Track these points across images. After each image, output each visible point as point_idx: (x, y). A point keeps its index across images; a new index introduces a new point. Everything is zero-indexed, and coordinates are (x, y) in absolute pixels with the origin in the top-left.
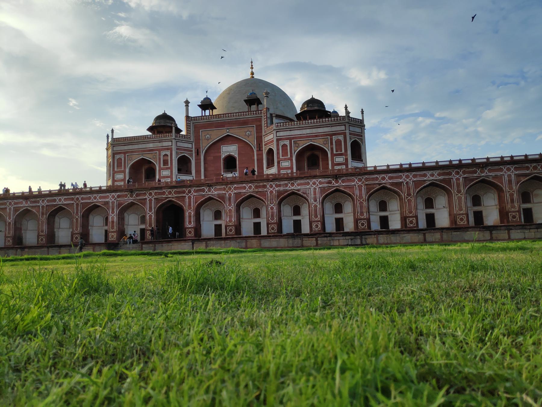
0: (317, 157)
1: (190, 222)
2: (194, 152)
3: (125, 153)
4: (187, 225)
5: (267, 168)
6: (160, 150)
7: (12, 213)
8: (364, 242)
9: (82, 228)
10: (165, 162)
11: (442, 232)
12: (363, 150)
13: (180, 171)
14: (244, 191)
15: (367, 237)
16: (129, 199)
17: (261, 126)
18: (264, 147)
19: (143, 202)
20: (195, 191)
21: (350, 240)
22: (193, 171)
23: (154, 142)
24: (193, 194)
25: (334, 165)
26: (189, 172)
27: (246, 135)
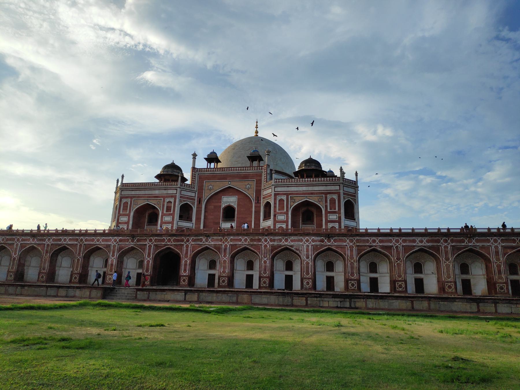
0: (313, 213)
1: (185, 270)
2: (196, 200)
3: (131, 198)
4: (182, 273)
5: (264, 220)
6: (164, 197)
8: (353, 306)
9: (82, 269)
11: (430, 301)
12: (355, 210)
13: (181, 217)
15: (356, 300)
16: (130, 244)
17: (261, 180)
18: (262, 200)
20: (193, 240)
21: (339, 302)
22: (194, 219)
23: (159, 189)
25: (327, 222)
26: (189, 219)
27: (246, 188)
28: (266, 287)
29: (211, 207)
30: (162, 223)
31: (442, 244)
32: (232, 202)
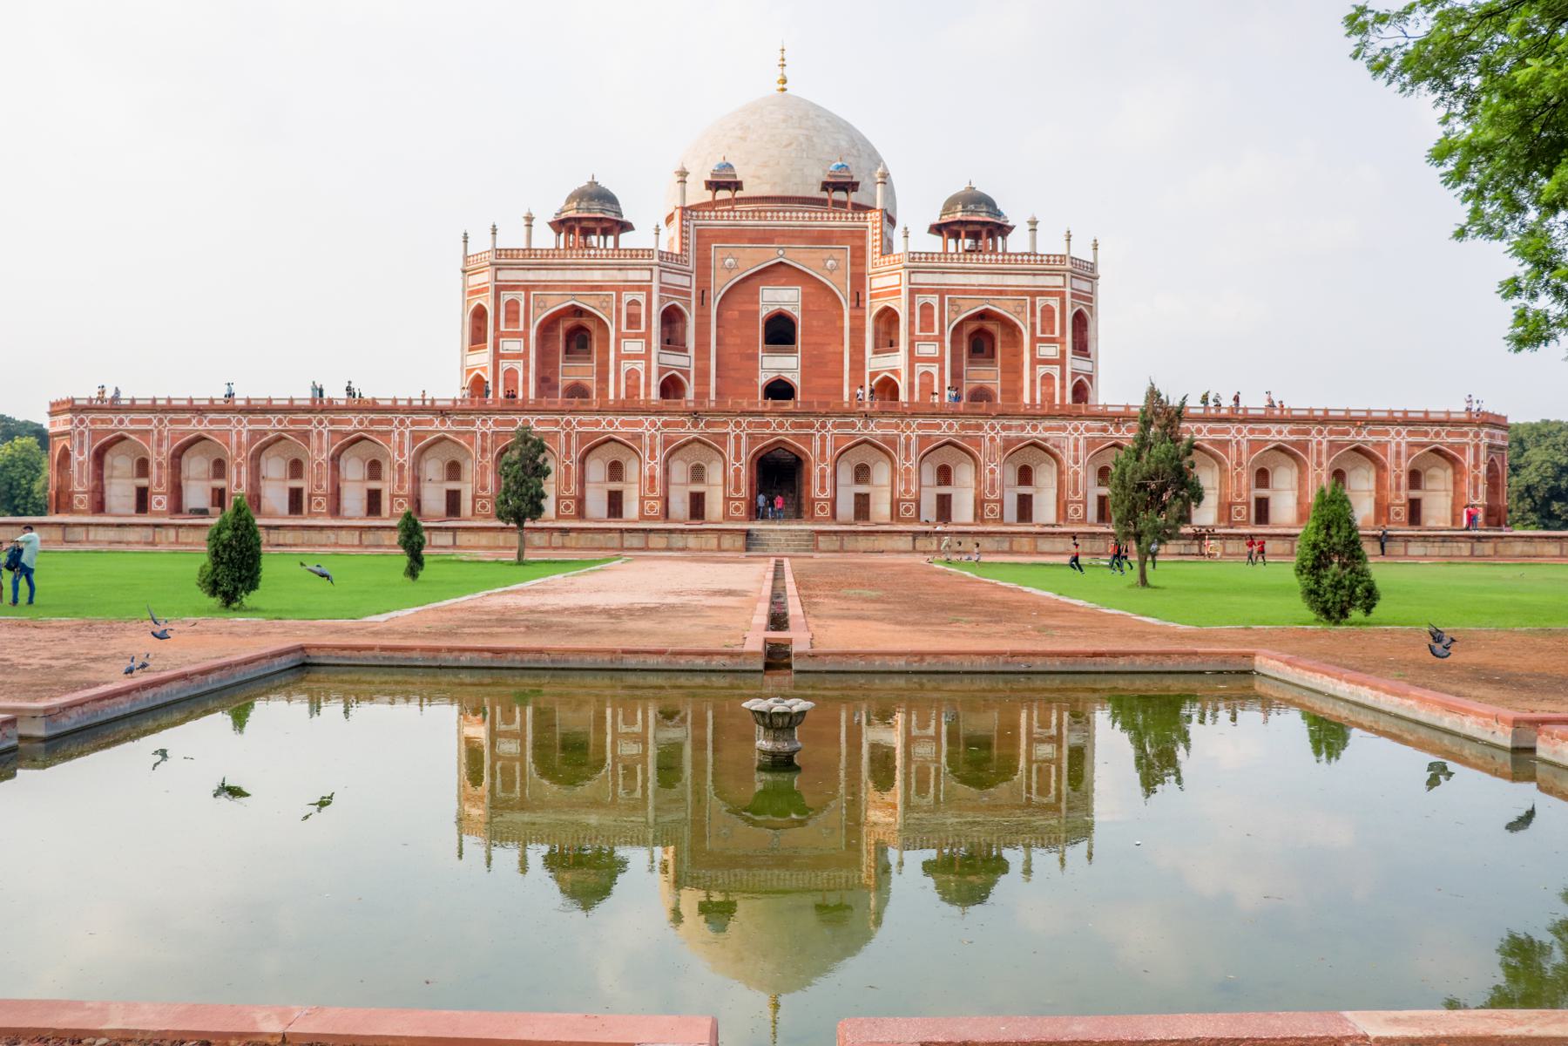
0: (991, 337)
1: (823, 489)
3: (527, 289)
4: (815, 492)
5: (875, 353)
6: (619, 290)
7: (407, 442)
10: (633, 321)
12: (1091, 333)
17: (863, 249)
18: (868, 301)
20: (835, 426)
23: (603, 267)
24: (831, 432)
25: (1035, 362)
26: (681, 347)
28: (995, 521)
29: (733, 314)
31: (1314, 438)
32: (788, 303)
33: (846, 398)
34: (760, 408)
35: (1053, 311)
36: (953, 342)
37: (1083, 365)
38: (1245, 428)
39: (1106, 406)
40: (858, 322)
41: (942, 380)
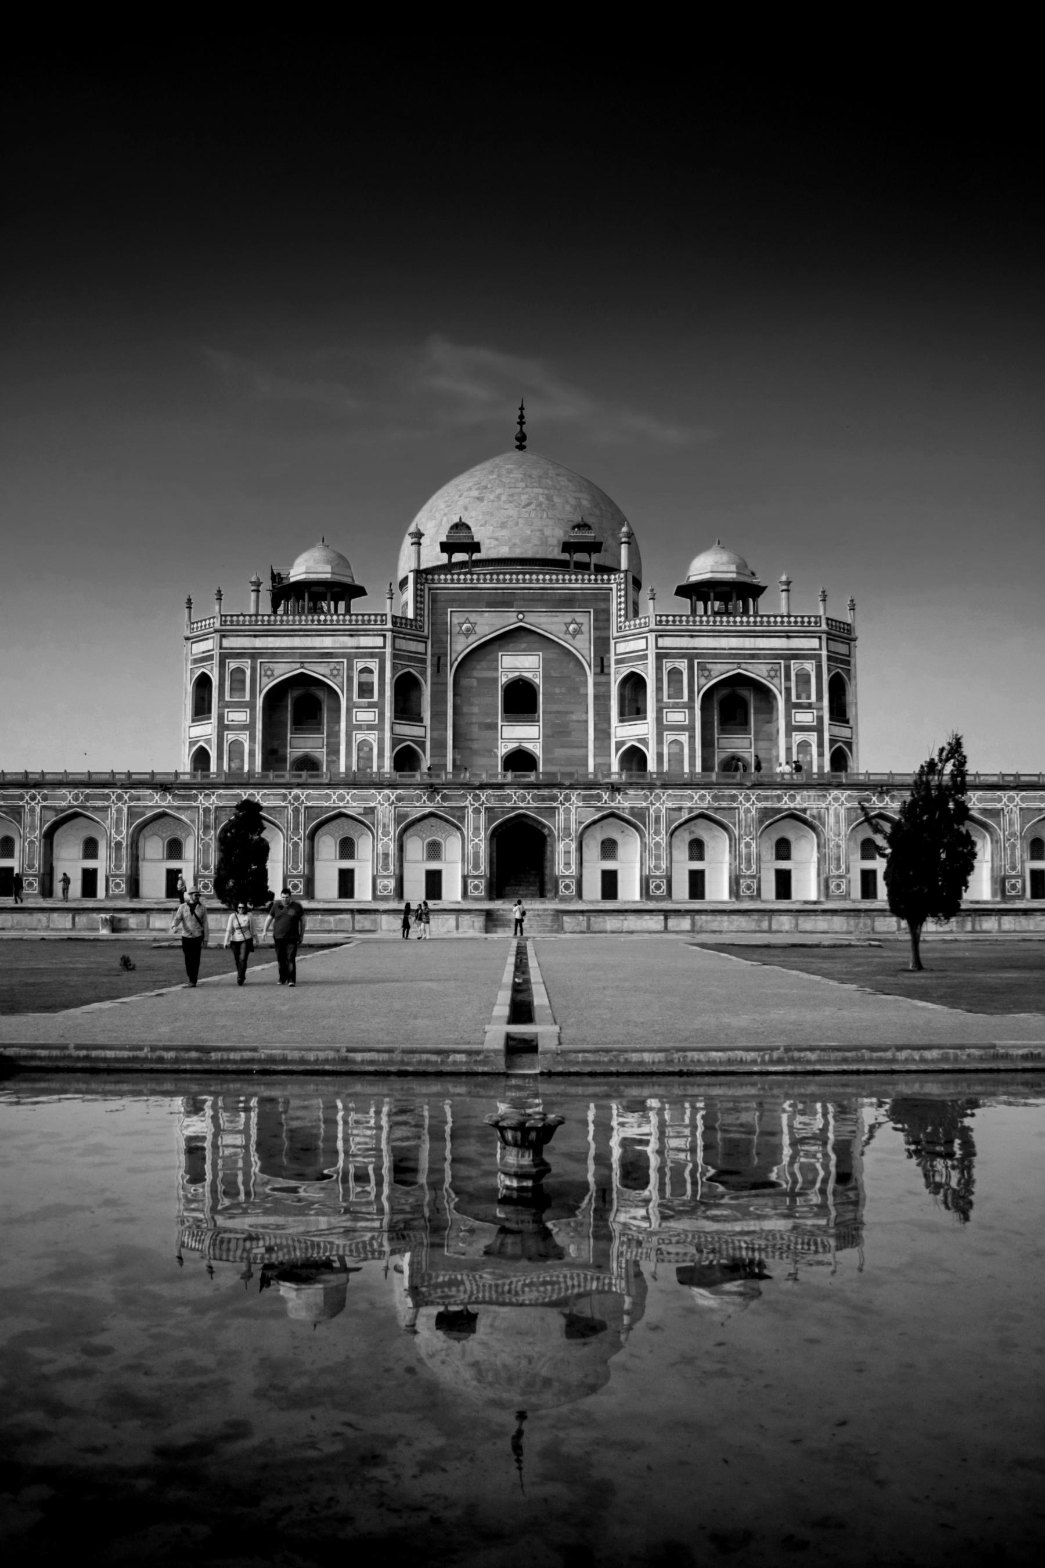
0: (744, 705)
1: (567, 864)
3: (253, 657)
4: (560, 869)
5: (621, 721)
6: (350, 657)
8: (978, 928)
10: (365, 689)
12: (849, 698)
14: (689, 805)
15: (983, 918)
17: (607, 612)
19: (459, 814)
23: (333, 633)
25: (791, 729)
26: (416, 718)
28: (751, 898)
30: (351, 728)
32: (529, 669)
33: (591, 769)
34: (500, 779)
35: (809, 676)
36: (702, 709)
37: (845, 732)
38: (1018, 796)
39: (868, 774)
40: (602, 689)
41: (692, 749)
